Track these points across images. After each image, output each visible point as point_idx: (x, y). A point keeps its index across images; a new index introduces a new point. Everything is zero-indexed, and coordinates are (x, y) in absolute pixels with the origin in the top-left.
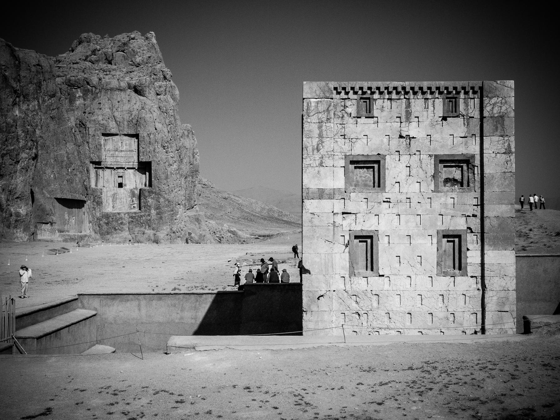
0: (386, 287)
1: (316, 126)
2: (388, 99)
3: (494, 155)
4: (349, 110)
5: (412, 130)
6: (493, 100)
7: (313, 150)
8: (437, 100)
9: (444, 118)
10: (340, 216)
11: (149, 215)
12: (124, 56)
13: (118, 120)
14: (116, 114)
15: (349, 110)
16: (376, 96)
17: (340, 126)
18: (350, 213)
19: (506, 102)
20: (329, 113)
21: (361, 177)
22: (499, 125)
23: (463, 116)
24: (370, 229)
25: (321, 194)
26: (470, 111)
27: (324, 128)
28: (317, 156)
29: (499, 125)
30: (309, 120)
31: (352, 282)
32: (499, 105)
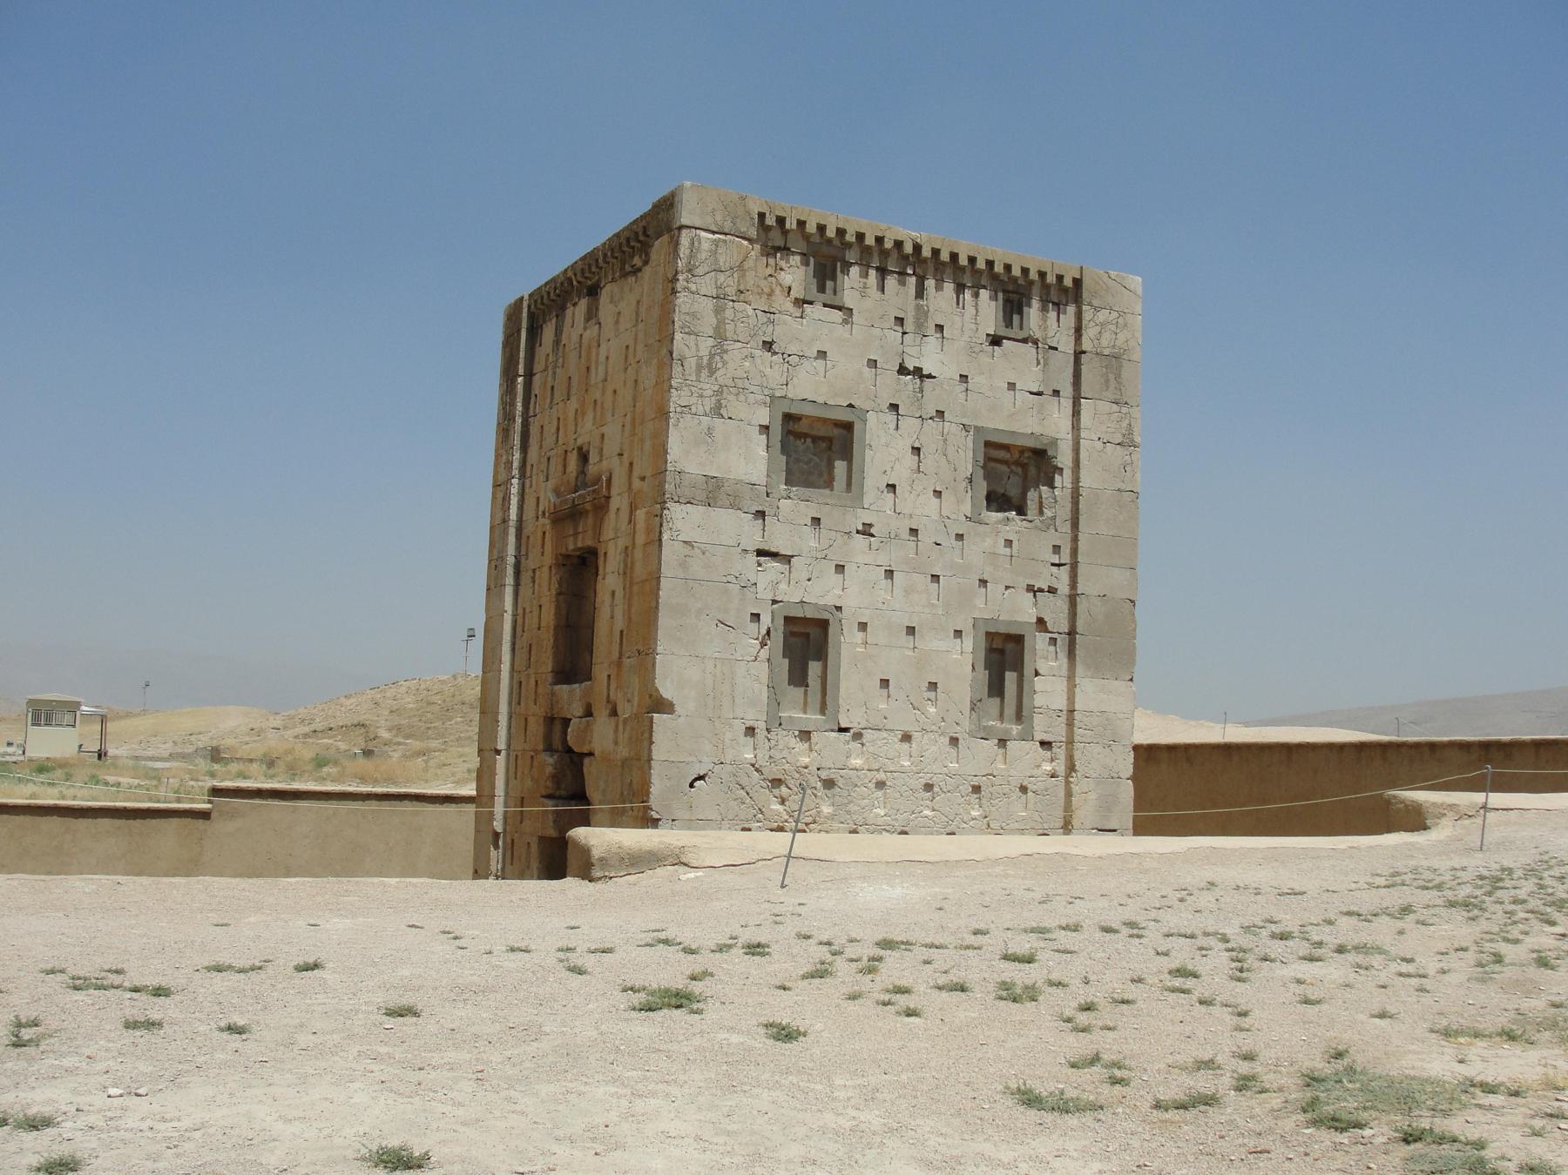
0: (857, 762)
4: (787, 278)
6: (1102, 316)
7: (699, 368)
9: (996, 341)
10: (753, 558)
17: (763, 318)
20: (744, 276)
22: (1111, 377)
23: (1035, 342)
25: (714, 493)
26: (1051, 334)
27: (729, 313)
28: (709, 387)
29: (1111, 377)
30: (693, 287)
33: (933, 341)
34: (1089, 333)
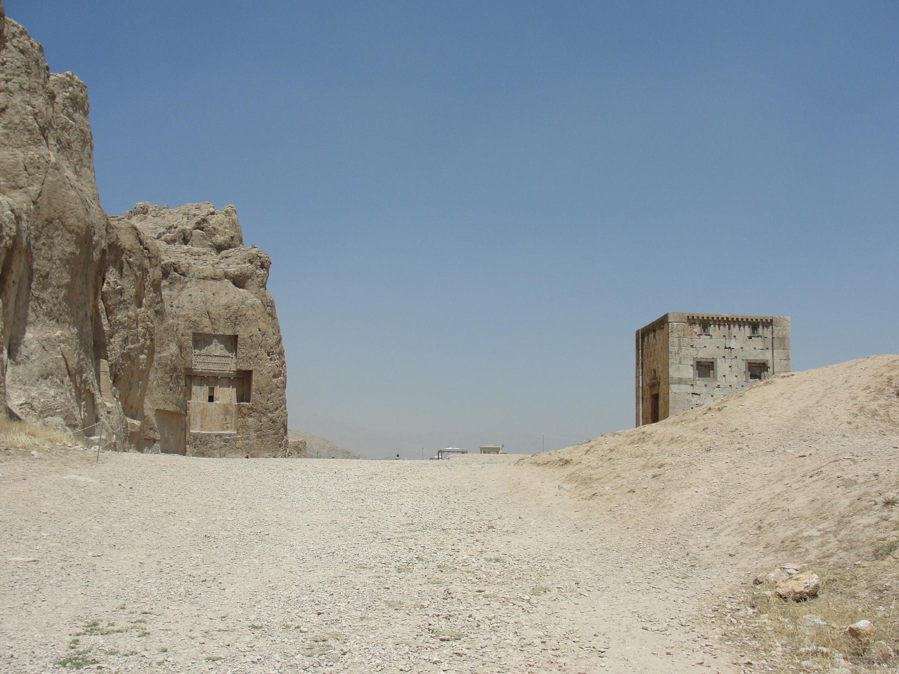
4: (695, 330)
5: (733, 344)
9: (750, 338)
11: (247, 438)
13: (212, 316)
14: (211, 309)
25: (680, 381)
28: (678, 358)
33: (733, 340)
34: (775, 333)
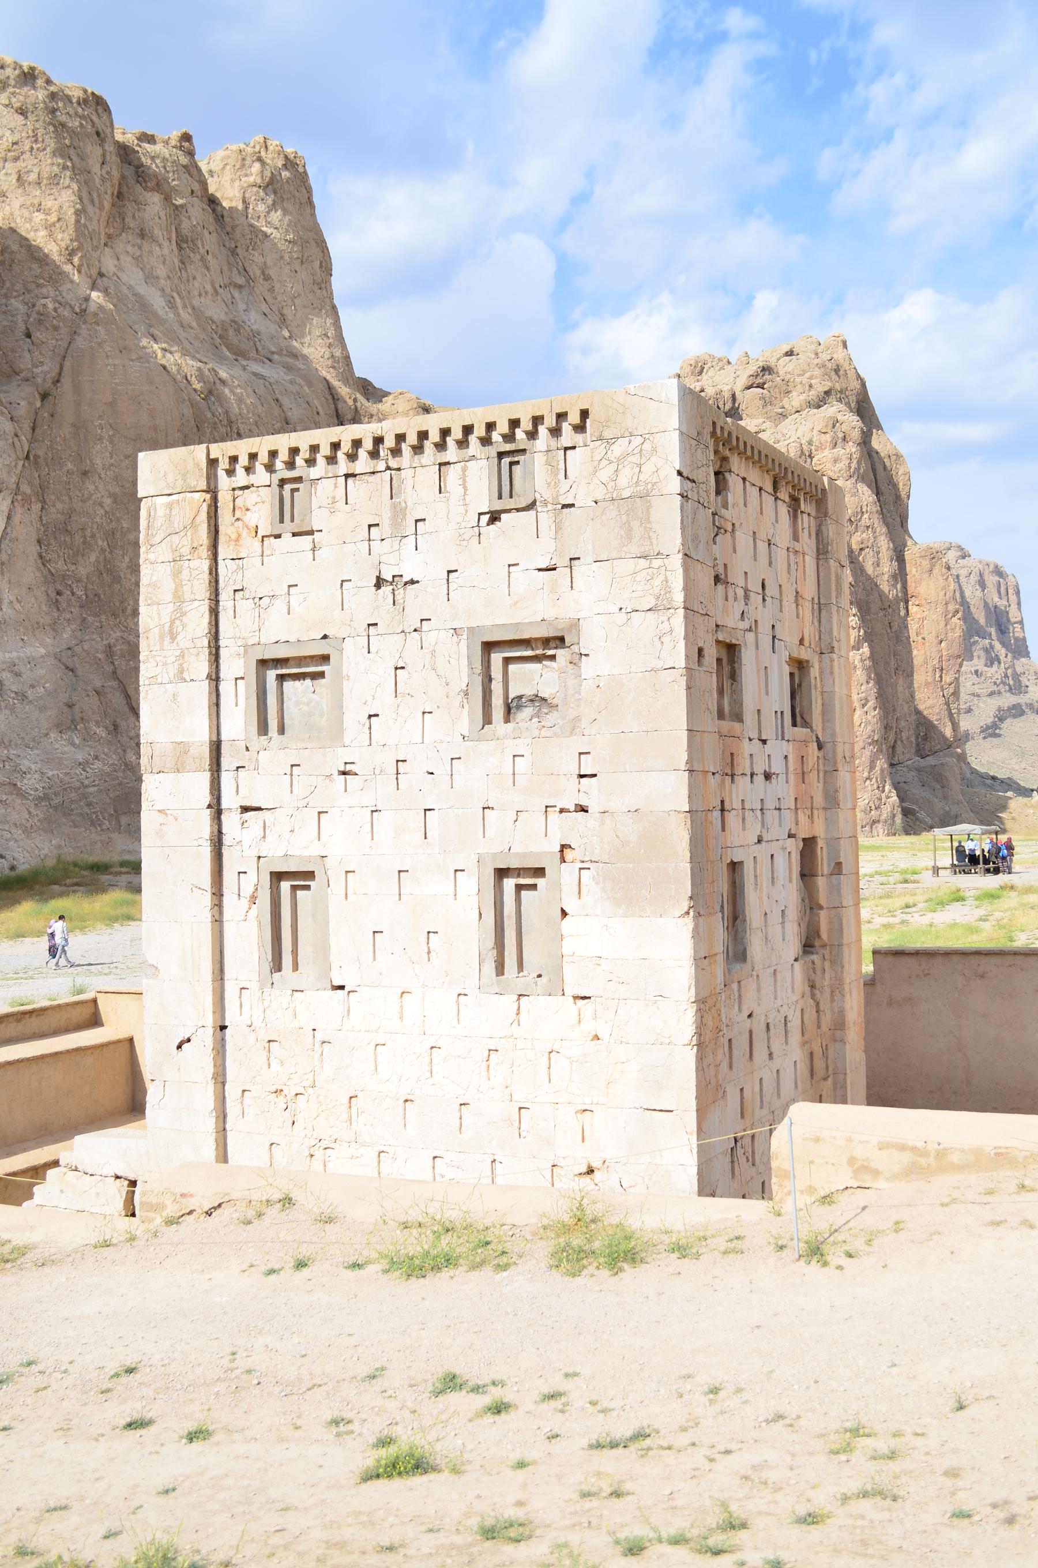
1: (168, 568)
2: (347, 476)
3: (622, 617)
4: (252, 518)
6: (618, 449)
8: (471, 464)
9: (494, 517)
12: (762, 398)
15: (252, 518)
16: (315, 472)
18: (259, 809)
19: (654, 450)
21: (298, 703)
22: (635, 524)
24: (306, 853)
27: (185, 574)
29: (635, 524)
30: (152, 556)
31: (266, 1004)
32: (635, 459)
